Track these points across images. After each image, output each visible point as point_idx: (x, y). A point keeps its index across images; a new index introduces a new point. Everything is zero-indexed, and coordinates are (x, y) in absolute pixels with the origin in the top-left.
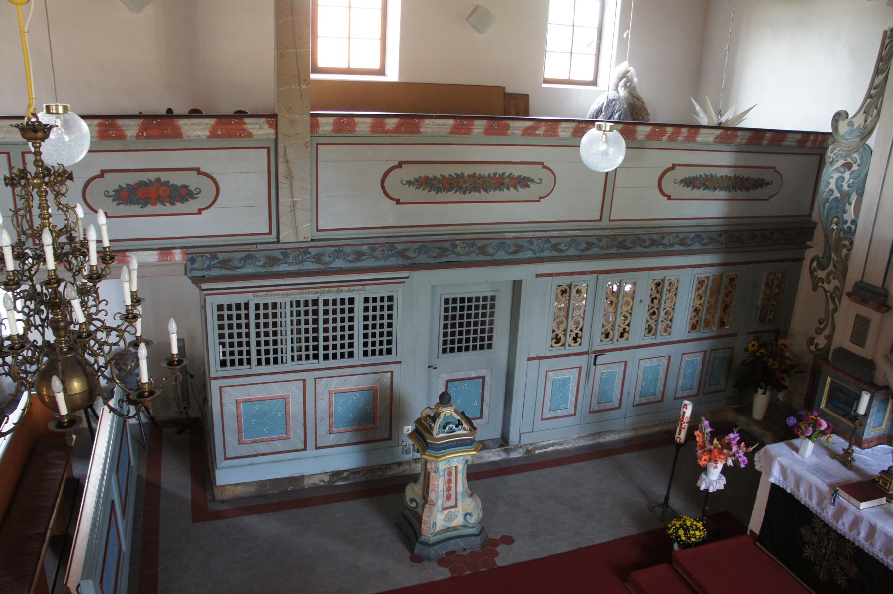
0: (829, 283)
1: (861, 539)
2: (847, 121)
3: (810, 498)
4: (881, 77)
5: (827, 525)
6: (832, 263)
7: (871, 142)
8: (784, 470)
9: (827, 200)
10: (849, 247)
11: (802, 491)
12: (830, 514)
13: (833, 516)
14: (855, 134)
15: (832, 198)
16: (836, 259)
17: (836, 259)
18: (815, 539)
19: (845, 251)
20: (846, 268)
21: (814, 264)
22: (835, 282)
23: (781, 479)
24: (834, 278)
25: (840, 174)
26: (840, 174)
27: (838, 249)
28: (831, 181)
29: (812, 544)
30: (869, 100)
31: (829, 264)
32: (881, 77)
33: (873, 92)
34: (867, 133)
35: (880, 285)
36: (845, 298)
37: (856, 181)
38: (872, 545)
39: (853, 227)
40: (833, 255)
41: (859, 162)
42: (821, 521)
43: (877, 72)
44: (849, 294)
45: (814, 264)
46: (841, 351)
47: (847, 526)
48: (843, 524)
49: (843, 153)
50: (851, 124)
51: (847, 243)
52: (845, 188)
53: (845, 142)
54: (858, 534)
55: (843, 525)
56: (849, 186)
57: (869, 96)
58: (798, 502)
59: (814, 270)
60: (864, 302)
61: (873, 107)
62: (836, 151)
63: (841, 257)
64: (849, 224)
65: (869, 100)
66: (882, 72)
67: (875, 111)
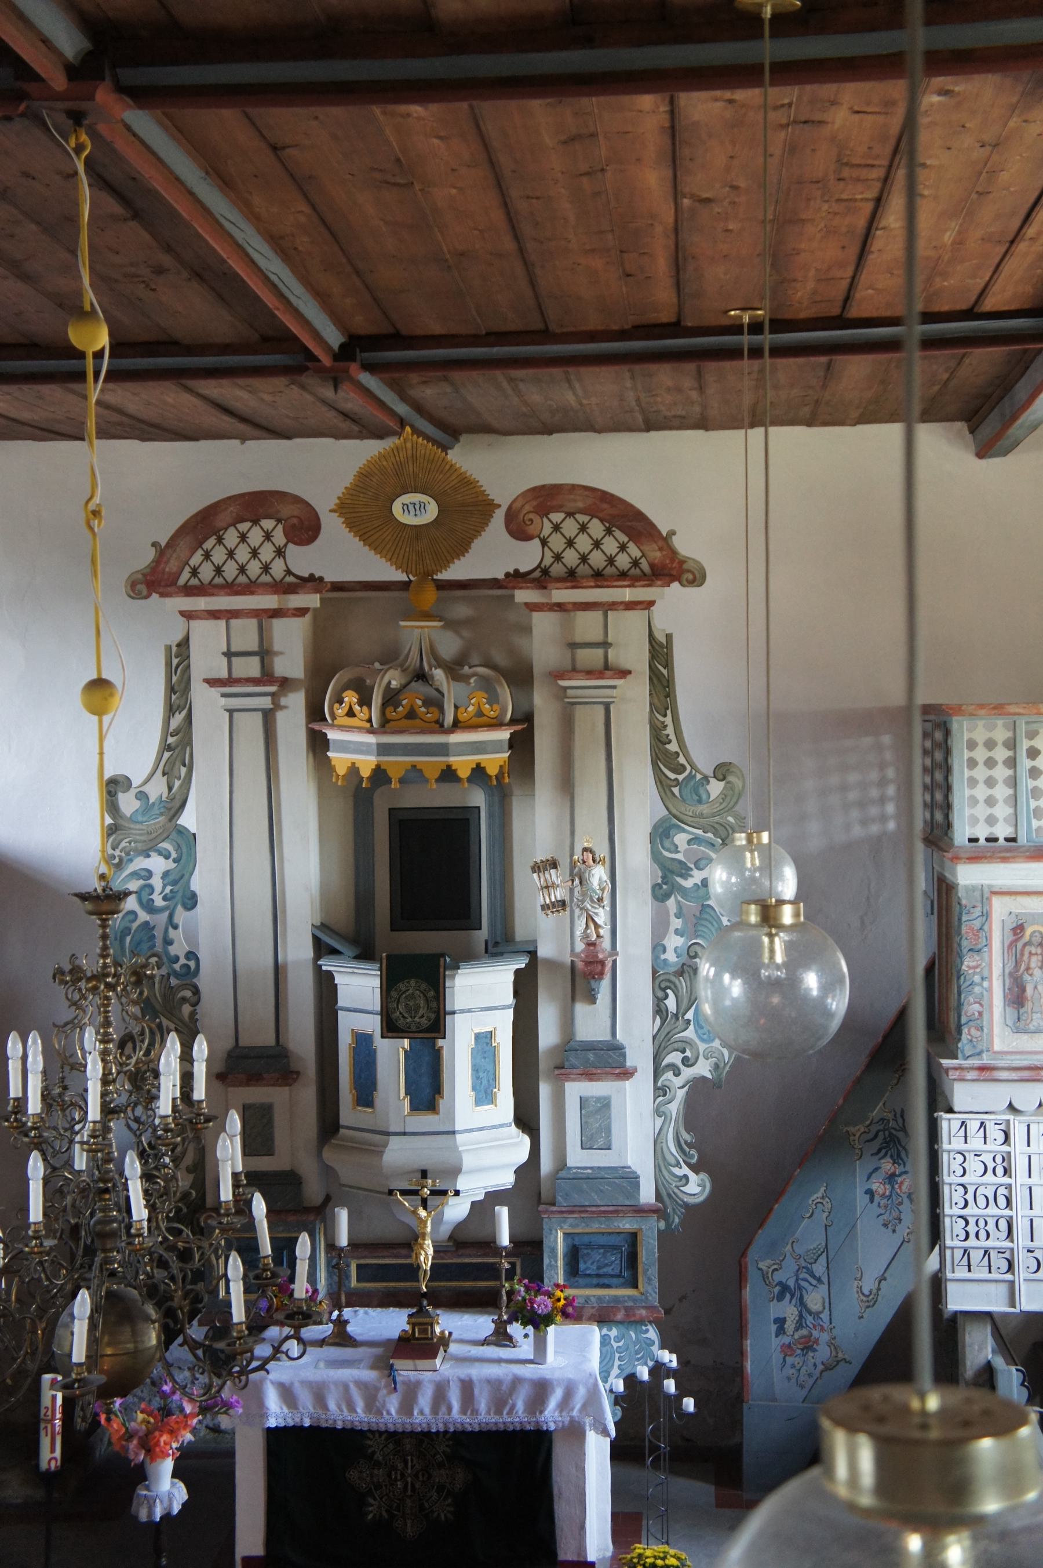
1: (456, 1416)
2: (133, 792)
3: (352, 1408)
4: (177, 720)
5: (395, 1433)
7: (188, 820)
8: (287, 1394)
9: (126, 931)
10: (194, 999)
11: (332, 1405)
12: (393, 1411)
13: (399, 1411)
14: (156, 811)
15: (135, 926)
18: (380, 1473)
19: (186, 1009)
23: (285, 1410)
25: (141, 882)
26: (141, 882)
29: (378, 1486)
30: (167, 755)
32: (177, 720)
33: (171, 740)
34: (177, 805)
35: (271, 1041)
37: (176, 888)
38: (475, 1412)
39: (192, 964)
41: (174, 855)
42: (381, 1433)
43: (171, 710)
47: (427, 1411)
48: (421, 1412)
49: (140, 846)
50: (142, 796)
51: (188, 994)
52: (159, 902)
53: (138, 826)
54: (450, 1409)
55: (423, 1415)
56: (165, 899)
57: (165, 747)
58: (332, 1431)
60: (254, 1078)
61: (178, 763)
62: (123, 844)
64: (183, 961)
65: (167, 755)
66: (180, 709)
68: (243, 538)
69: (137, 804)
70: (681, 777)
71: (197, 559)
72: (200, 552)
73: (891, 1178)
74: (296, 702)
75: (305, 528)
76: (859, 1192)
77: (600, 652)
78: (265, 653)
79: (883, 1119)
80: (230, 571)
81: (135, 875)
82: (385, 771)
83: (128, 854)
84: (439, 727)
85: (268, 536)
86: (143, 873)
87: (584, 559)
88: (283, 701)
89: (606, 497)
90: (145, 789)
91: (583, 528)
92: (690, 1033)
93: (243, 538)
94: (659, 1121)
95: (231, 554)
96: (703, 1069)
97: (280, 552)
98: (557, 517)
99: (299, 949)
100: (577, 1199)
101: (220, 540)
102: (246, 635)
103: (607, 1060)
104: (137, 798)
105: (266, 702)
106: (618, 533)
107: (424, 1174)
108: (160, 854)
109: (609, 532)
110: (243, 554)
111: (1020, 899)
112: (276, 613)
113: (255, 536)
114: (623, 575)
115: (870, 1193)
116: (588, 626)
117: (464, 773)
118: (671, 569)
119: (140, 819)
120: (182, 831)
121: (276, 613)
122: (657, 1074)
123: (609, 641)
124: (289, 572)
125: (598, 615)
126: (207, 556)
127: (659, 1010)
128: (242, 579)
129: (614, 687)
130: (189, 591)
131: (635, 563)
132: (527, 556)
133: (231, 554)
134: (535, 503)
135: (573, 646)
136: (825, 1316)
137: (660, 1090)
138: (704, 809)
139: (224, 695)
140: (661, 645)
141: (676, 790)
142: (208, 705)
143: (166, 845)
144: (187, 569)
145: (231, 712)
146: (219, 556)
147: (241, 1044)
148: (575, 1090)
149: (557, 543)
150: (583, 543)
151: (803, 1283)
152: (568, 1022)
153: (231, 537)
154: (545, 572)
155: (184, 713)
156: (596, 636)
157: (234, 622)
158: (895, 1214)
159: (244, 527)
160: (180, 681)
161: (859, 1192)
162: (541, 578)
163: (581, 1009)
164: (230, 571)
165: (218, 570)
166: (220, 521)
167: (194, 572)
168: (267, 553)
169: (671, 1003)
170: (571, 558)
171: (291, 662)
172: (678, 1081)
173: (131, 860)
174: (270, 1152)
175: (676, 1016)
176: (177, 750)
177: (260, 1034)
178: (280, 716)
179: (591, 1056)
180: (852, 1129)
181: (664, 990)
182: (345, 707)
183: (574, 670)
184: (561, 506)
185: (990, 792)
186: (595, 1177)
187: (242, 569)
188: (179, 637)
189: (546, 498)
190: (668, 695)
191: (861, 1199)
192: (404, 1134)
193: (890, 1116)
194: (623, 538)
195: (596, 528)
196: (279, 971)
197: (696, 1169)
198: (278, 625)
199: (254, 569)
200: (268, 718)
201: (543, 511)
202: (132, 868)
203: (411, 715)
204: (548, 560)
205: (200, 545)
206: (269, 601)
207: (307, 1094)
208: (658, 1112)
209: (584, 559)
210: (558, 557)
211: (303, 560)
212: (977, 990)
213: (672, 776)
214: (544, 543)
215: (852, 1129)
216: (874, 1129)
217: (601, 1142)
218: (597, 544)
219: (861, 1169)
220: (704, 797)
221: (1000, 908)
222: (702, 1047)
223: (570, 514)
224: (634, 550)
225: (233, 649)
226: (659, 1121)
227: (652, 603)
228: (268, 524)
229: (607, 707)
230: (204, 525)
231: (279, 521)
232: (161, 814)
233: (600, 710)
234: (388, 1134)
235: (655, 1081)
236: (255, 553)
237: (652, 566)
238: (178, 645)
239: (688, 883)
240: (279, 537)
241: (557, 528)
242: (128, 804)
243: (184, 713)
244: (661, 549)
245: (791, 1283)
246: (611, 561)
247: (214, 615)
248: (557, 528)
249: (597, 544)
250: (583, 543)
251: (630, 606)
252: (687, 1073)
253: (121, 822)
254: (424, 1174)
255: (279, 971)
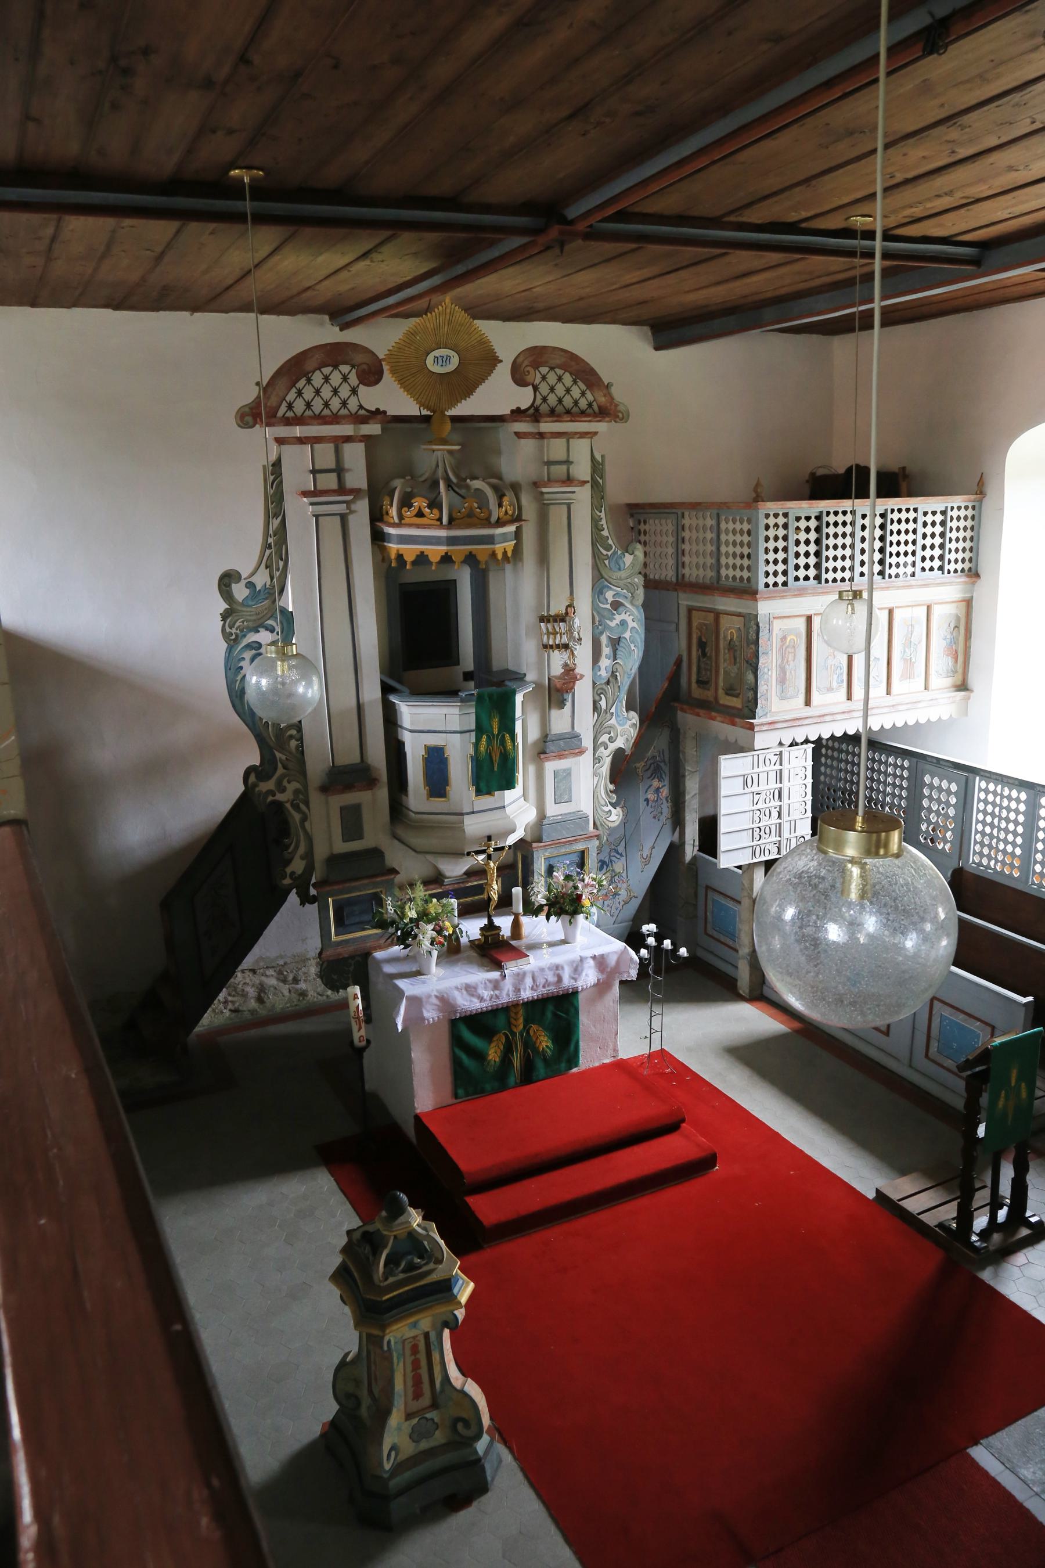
0: (283, 790)
2: (243, 583)
6: (280, 765)
10: (298, 736)
16: (284, 757)
17: (284, 757)
19: (293, 743)
20: (302, 762)
21: (252, 778)
22: (292, 787)
24: (289, 782)
25: (254, 652)
27: (282, 746)
28: (242, 664)
30: (268, 552)
31: (276, 769)
32: (276, 523)
36: (316, 799)
40: (278, 755)
44: (325, 789)
45: (252, 778)
46: (334, 860)
49: (251, 624)
50: (250, 585)
51: (294, 732)
59: (255, 785)
60: (349, 787)
62: (238, 624)
63: (291, 753)
67: (281, 563)
68: (326, 379)
69: (247, 592)
70: (609, 553)
71: (292, 395)
72: (294, 390)
73: (657, 790)
74: (362, 507)
75: (371, 375)
76: (642, 800)
77: (564, 467)
78: (339, 470)
79: (654, 757)
80: (317, 406)
81: (249, 646)
82: (475, 556)
83: (242, 631)
84: (487, 523)
85: (345, 378)
86: (255, 645)
87: (560, 401)
88: (353, 507)
89: (573, 357)
90: (252, 579)
91: (560, 379)
92: (613, 721)
93: (326, 379)
94: (596, 779)
95: (318, 392)
96: (620, 743)
97: (354, 391)
98: (544, 370)
99: (372, 692)
100: (555, 836)
101: (309, 381)
102: (326, 455)
103: (570, 745)
104: (246, 587)
105: (342, 508)
106: (580, 383)
107: (489, 838)
108: (267, 629)
109: (575, 382)
110: (326, 393)
111: (785, 621)
112: (348, 439)
113: (336, 378)
114: (583, 413)
115: (647, 800)
116: (556, 449)
117: (435, 559)
118: (606, 412)
119: (250, 603)
120: (284, 611)
121: (348, 439)
122: (595, 750)
123: (571, 459)
124: (361, 407)
125: (561, 442)
126: (300, 393)
127: (596, 707)
128: (326, 412)
129: (574, 492)
130: (288, 422)
131: (590, 405)
132: (524, 398)
133: (318, 392)
134: (531, 359)
135: (549, 463)
136: (624, 875)
137: (597, 760)
138: (623, 574)
139: (312, 504)
140: (598, 462)
141: (607, 562)
142: (299, 512)
143: (270, 622)
144: (284, 404)
145: (317, 516)
146: (308, 393)
147: (336, 764)
148: (551, 767)
149: (544, 389)
150: (560, 390)
151: (613, 859)
152: (545, 723)
153: (317, 379)
154: (537, 409)
155: (280, 518)
156: (561, 455)
157: (316, 446)
158: (659, 810)
159: (327, 370)
160: (275, 493)
161: (642, 800)
162: (533, 414)
163: (555, 713)
164: (317, 406)
165: (308, 405)
166: (310, 365)
167: (290, 406)
168: (345, 392)
169: (603, 703)
170: (552, 400)
171: (357, 477)
172: (607, 752)
173: (245, 636)
174: (360, 836)
175: (606, 711)
176: (276, 547)
177: (350, 756)
178: (351, 518)
179: (562, 743)
180: (638, 765)
181: (599, 695)
182: (414, 510)
183: (550, 482)
184: (547, 362)
185: (776, 556)
186: (563, 822)
187: (326, 405)
188: (273, 457)
189: (537, 356)
190: (602, 498)
191: (642, 804)
192: (473, 813)
193: (657, 754)
194: (583, 387)
195: (568, 379)
196: (359, 707)
197: (614, 805)
198: (348, 449)
199: (335, 404)
200: (344, 518)
201: (536, 366)
202: (245, 642)
203: (420, 514)
204: (539, 401)
205: (294, 385)
206: (347, 429)
207: (383, 793)
208: (595, 774)
209: (560, 401)
210: (545, 399)
211: (372, 397)
212: (766, 676)
213: (605, 552)
214: (536, 388)
215: (638, 765)
216: (649, 762)
217: (566, 798)
218: (568, 391)
219: (642, 787)
220: (622, 566)
221: (777, 625)
222: (619, 729)
223: (552, 369)
224: (589, 396)
225: (317, 468)
226: (596, 779)
227: (596, 433)
228: (345, 369)
229: (569, 506)
230: (295, 369)
231: (353, 366)
232: (266, 599)
233: (565, 507)
234: (462, 814)
235: (594, 754)
236: (335, 391)
237: (599, 407)
238: (273, 465)
239: (613, 624)
240: (353, 380)
241: (544, 378)
242: (240, 592)
243: (280, 518)
244: (605, 396)
245: (607, 860)
246: (576, 403)
247: (301, 441)
248: (544, 378)
249: (568, 391)
250: (560, 390)
251: (583, 435)
252: (613, 747)
253: (235, 606)
254: (489, 838)
255: (359, 707)
